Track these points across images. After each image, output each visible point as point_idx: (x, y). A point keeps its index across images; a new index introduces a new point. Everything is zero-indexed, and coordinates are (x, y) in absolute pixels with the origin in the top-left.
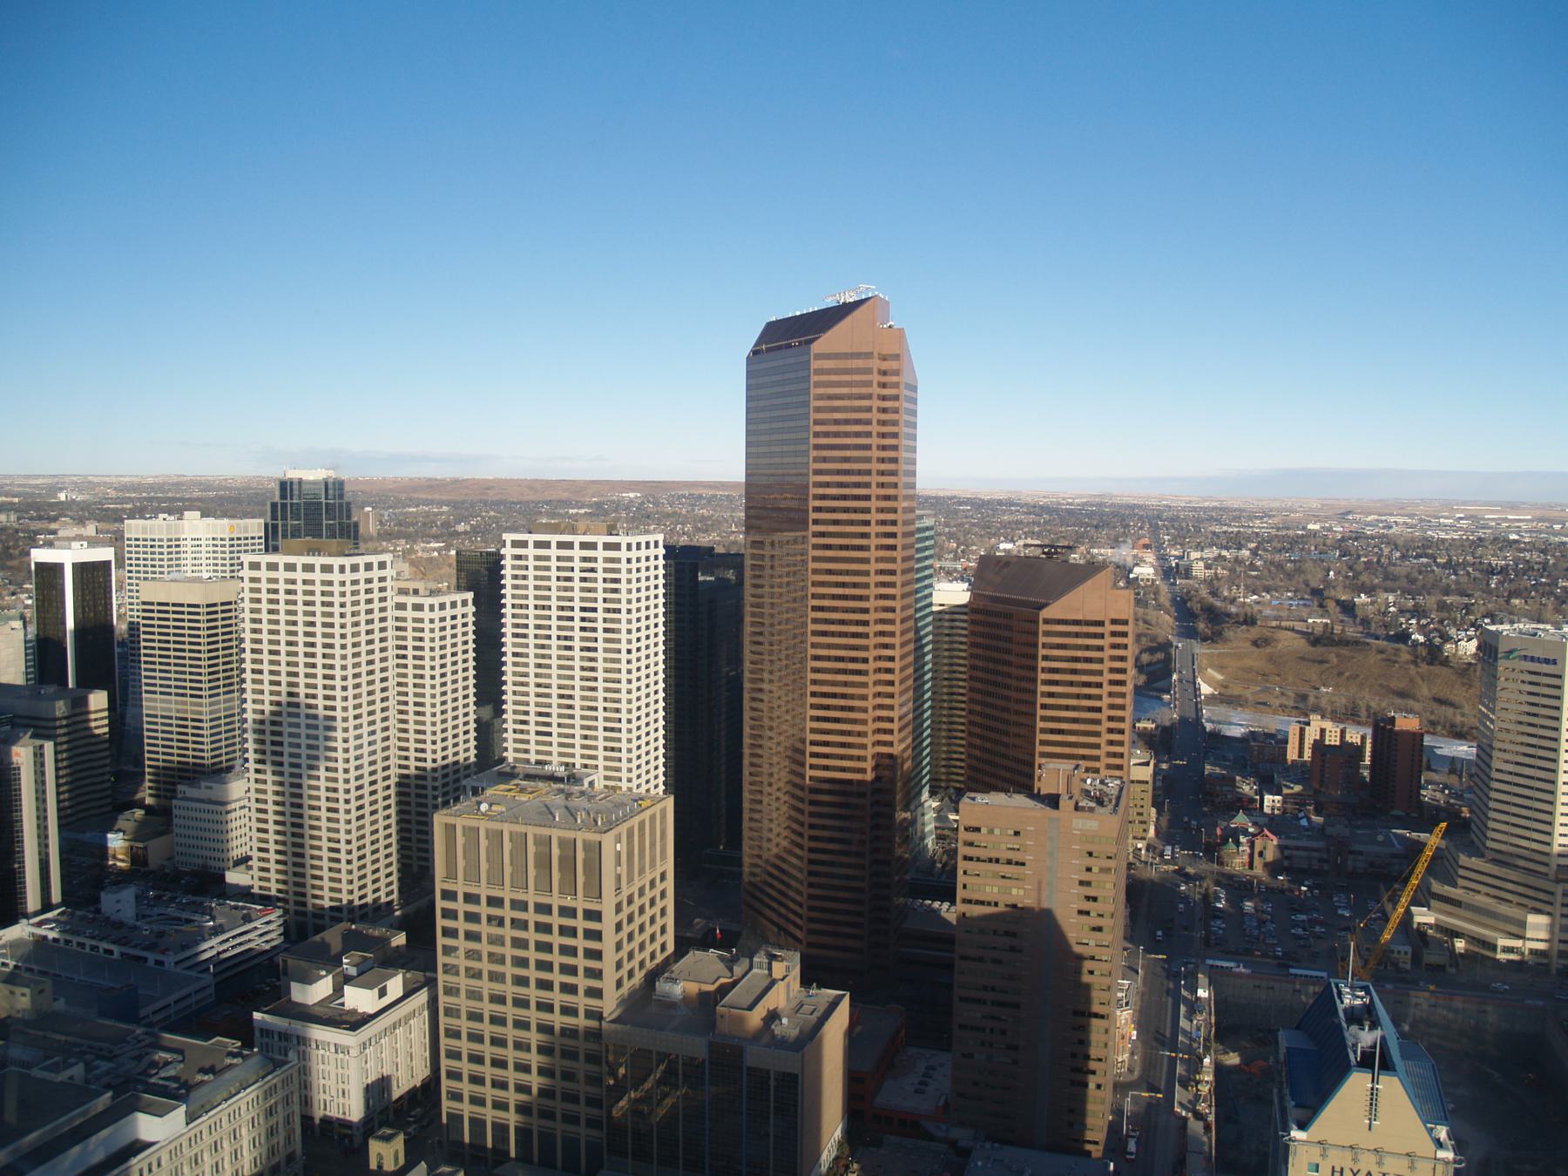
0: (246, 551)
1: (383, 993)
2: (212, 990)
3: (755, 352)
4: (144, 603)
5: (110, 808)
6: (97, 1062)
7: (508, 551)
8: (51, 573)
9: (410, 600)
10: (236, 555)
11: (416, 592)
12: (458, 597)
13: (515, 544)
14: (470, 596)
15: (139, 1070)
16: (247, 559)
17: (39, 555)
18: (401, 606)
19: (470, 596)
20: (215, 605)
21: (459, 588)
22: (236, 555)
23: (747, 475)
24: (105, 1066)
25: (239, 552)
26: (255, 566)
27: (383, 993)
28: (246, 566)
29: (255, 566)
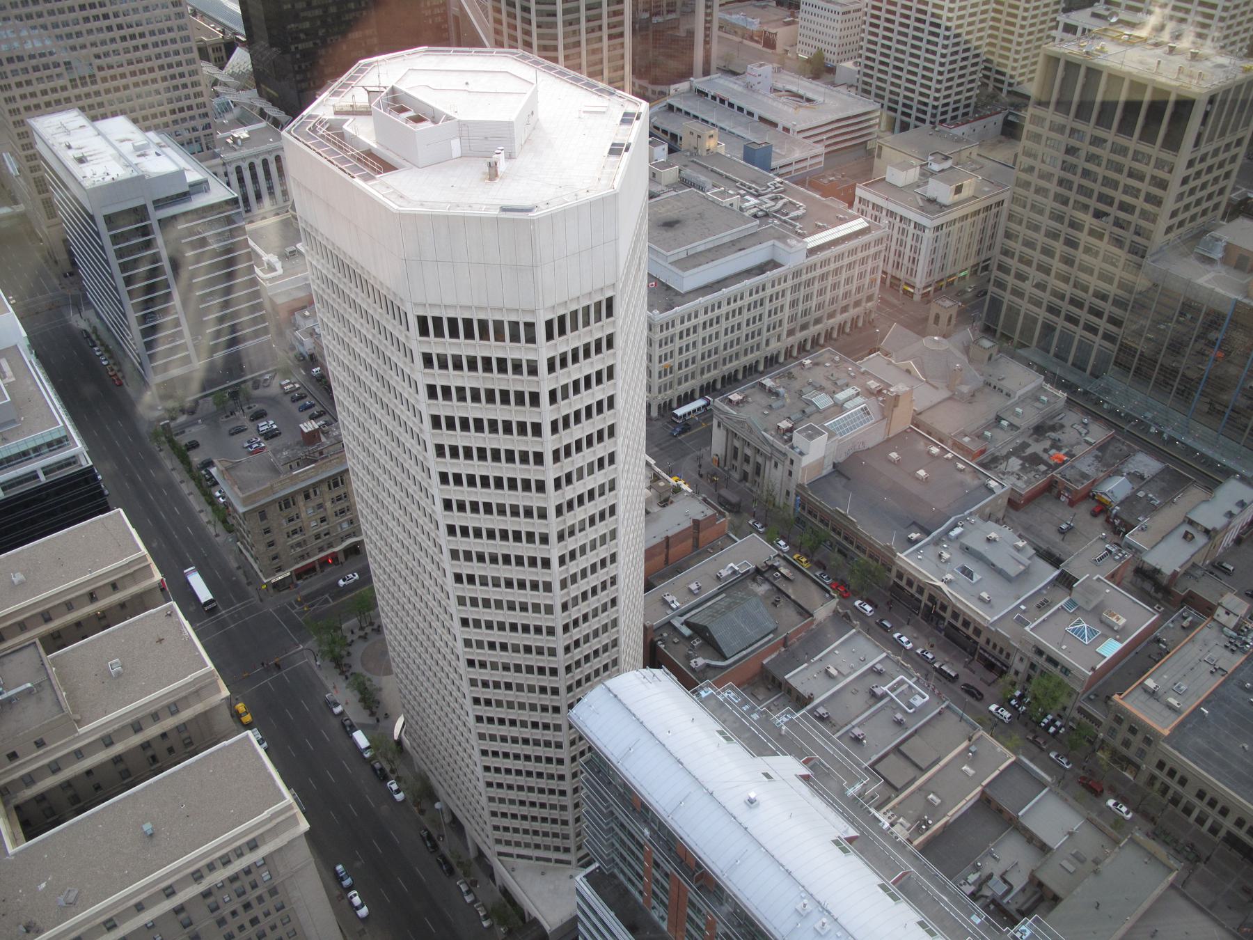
1: (958, 190)
2: (822, 159)
6: (747, 197)
15: (774, 208)
24: (753, 201)
27: (958, 190)
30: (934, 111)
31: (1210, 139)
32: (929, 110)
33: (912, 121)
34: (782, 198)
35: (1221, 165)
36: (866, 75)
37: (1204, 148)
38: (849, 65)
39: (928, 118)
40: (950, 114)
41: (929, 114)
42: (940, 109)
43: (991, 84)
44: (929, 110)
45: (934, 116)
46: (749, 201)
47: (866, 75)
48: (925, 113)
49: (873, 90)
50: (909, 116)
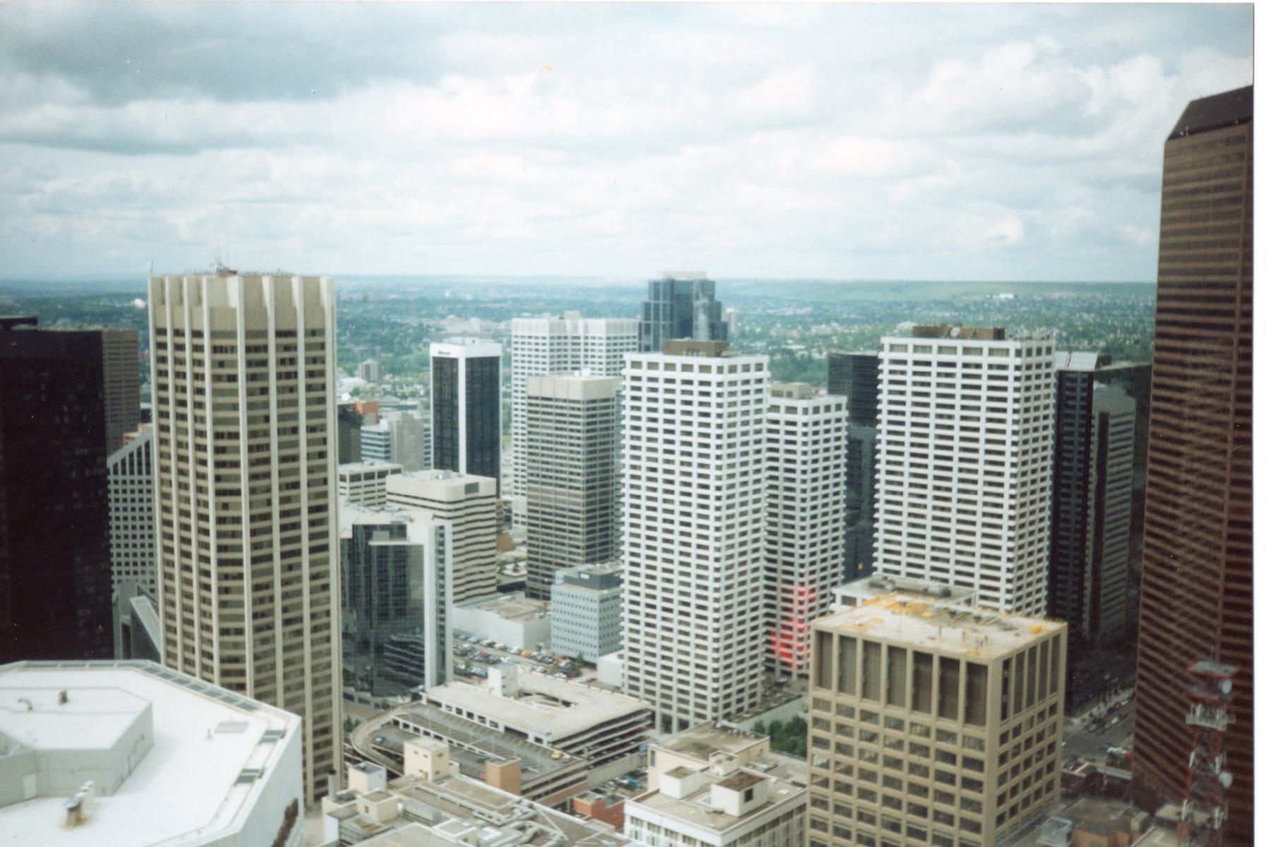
0: (628, 350)
3: (1174, 136)
4: (530, 398)
5: (494, 589)
7: (885, 355)
8: (445, 367)
9: (783, 402)
10: (618, 353)
11: (790, 395)
12: (833, 400)
13: (893, 348)
14: (843, 400)
16: (629, 357)
17: (436, 350)
18: (775, 408)
19: (843, 400)
20: (594, 401)
21: (832, 391)
22: (618, 353)
23: (1161, 272)
25: (621, 350)
26: (636, 365)
28: (628, 364)
29: (636, 365)
30: (715, 705)
31: (1018, 709)
32: (709, 703)
33: (690, 718)
34: (531, 826)
35: (1040, 737)
36: (632, 668)
37: (1013, 721)
38: (612, 658)
39: (709, 713)
40: (733, 709)
41: (709, 708)
42: (722, 702)
43: (778, 668)
44: (709, 703)
45: (715, 710)
46: (488, 833)
47: (632, 668)
48: (704, 707)
49: (641, 685)
50: (686, 712)
